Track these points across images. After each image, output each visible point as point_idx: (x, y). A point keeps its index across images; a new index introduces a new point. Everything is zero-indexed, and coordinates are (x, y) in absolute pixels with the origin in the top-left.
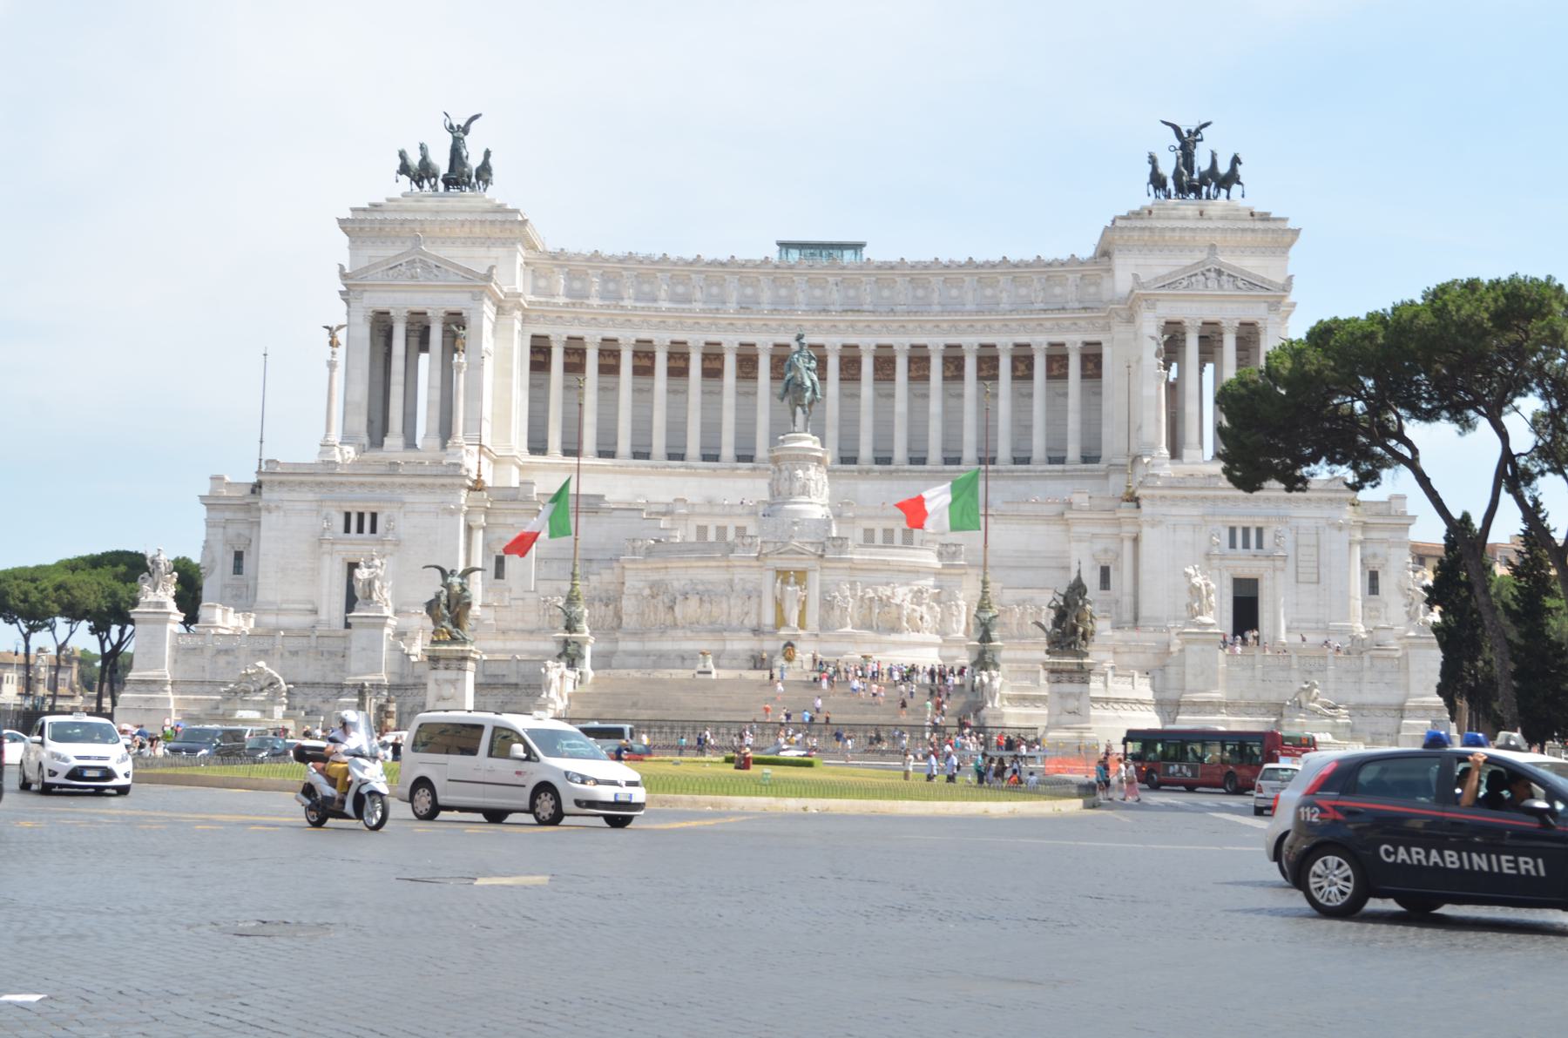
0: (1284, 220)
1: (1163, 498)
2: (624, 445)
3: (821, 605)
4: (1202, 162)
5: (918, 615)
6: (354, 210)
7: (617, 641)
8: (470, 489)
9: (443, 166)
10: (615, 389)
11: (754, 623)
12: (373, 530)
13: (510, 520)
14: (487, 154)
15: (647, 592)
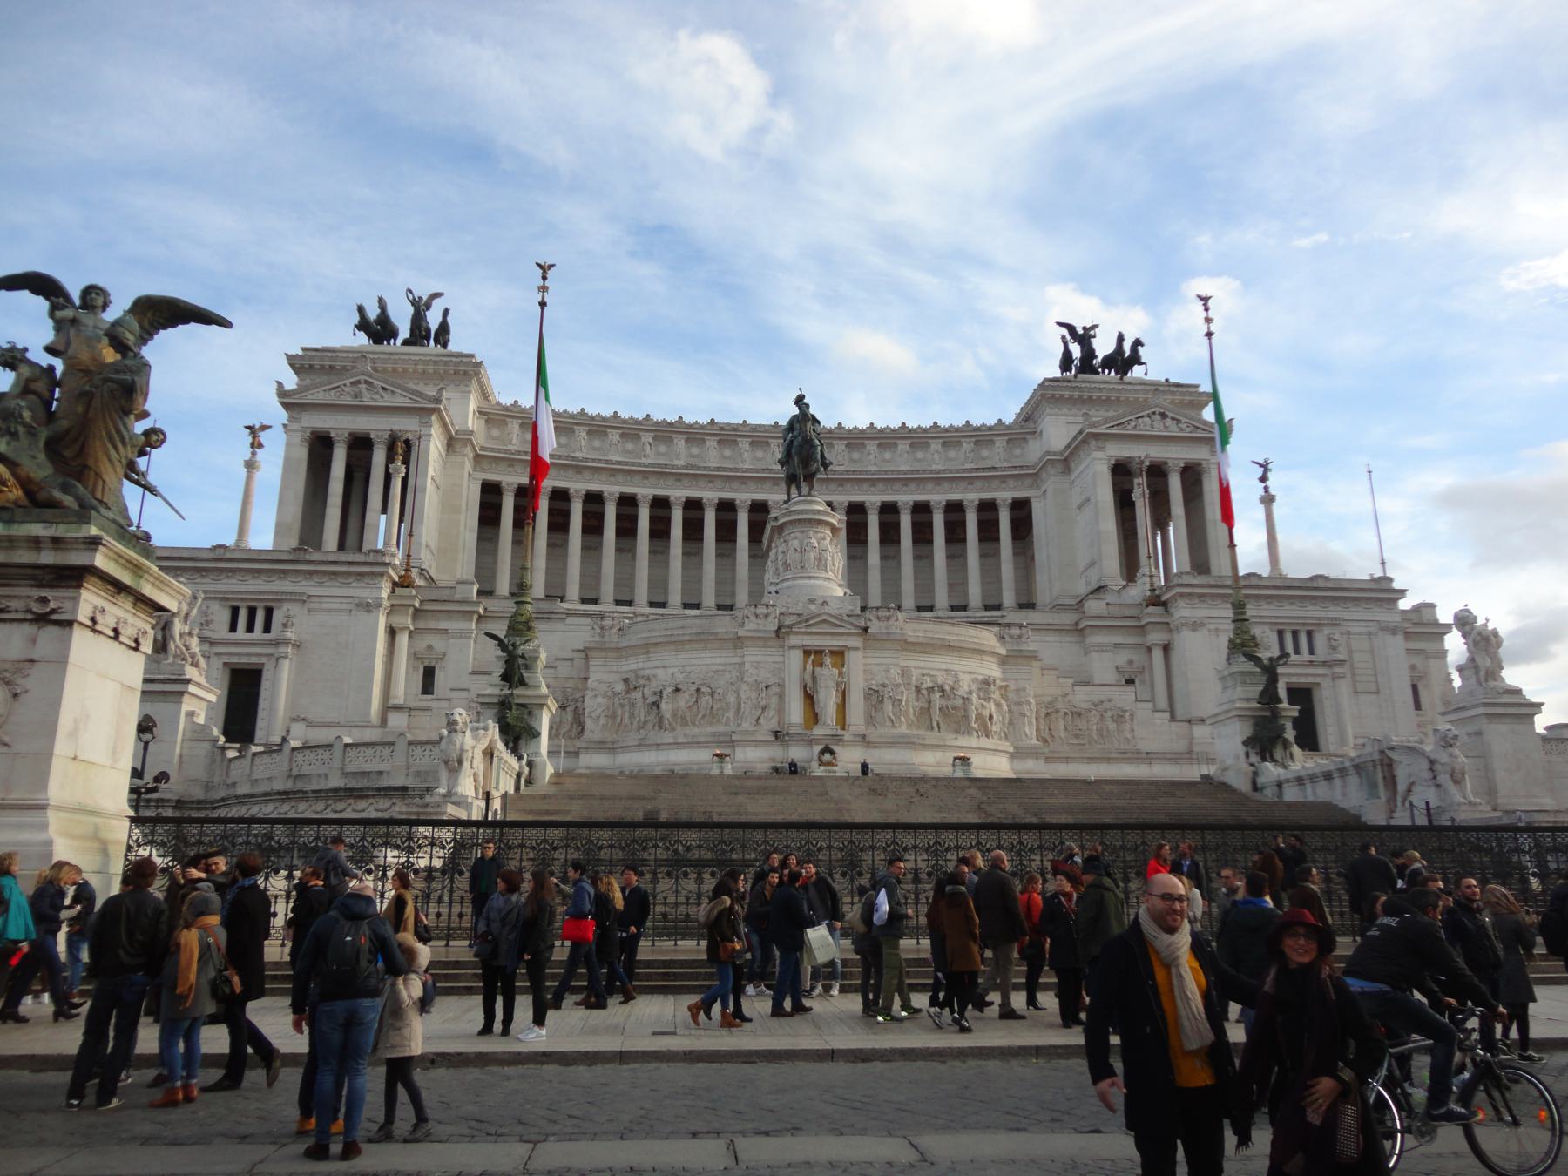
0: (1197, 386)
1: (1201, 596)
2: (573, 590)
3: (867, 697)
4: (1103, 346)
5: (986, 713)
6: (304, 349)
7: (576, 754)
8: (395, 584)
9: (404, 332)
10: (564, 544)
11: (773, 725)
12: (267, 629)
13: (443, 625)
14: (446, 312)
15: (620, 687)
